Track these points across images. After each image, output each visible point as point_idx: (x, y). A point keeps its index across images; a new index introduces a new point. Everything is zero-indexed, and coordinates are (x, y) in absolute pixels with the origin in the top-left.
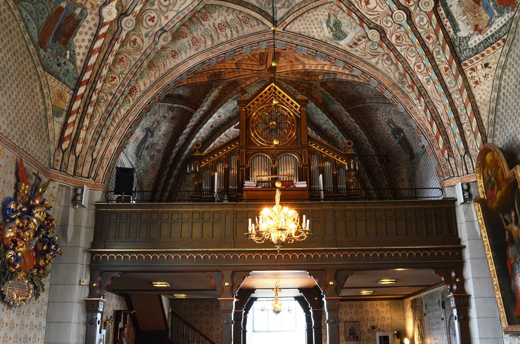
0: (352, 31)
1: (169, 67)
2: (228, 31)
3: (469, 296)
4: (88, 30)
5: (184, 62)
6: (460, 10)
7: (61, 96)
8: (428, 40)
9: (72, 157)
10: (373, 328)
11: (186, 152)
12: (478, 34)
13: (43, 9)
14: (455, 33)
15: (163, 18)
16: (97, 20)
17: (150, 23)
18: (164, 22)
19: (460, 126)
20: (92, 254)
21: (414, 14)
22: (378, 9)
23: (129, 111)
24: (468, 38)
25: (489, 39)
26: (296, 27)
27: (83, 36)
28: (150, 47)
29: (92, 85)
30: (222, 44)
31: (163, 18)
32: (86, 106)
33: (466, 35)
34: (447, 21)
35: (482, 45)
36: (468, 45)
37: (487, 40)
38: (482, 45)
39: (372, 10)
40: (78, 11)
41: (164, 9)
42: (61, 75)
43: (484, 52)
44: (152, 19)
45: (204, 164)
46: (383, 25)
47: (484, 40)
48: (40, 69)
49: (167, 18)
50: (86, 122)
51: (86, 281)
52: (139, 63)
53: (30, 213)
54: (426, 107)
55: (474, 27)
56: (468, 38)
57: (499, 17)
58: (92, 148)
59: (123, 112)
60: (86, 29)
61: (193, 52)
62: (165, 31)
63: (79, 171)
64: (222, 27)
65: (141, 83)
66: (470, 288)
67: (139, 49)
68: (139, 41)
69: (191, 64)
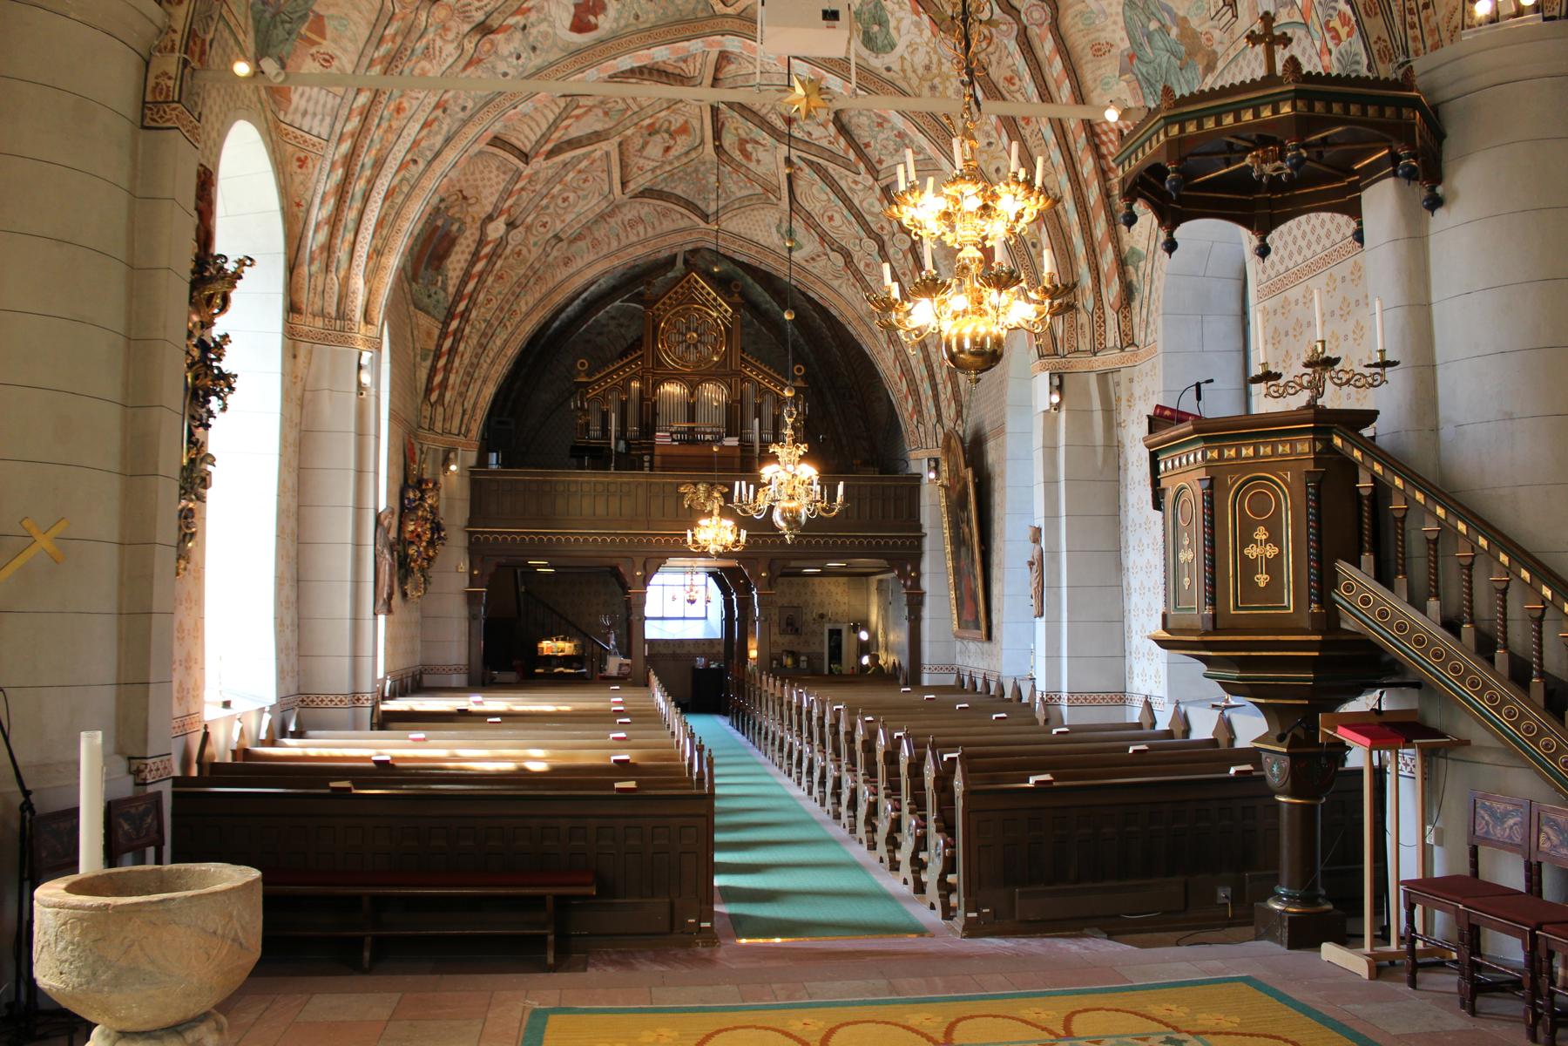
0: (809, 245)
1: (559, 278)
2: (641, 228)
3: (922, 594)
5: (579, 272)
7: (429, 334)
10: (822, 616)
16: (477, 237)
17: (542, 230)
18: (559, 226)
19: (934, 387)
20: (471, 534)
21: (888, 244)
23: (506, 342)
26: (733, 224)
28: (538, 259)
29: (465, 316)
30: (631, 245)
32: (456, 342)
40: (455, 227)
42: (431, 309)
45: (591, 394)
46: (850, 247)
48: (412, 308)
50: (456, 363)
51: (464, 566)
52: (524, 281)
53: (422, 499)
54: (896, 357)
58: (463, 395)
59: (499, 342)
61: (592, 257)
63: (448, 426)
64: (632, 224)
65: (522, 303)
66: (926, 584)
67: (524, 261)
68: (525, 251)
69: (589, 274)
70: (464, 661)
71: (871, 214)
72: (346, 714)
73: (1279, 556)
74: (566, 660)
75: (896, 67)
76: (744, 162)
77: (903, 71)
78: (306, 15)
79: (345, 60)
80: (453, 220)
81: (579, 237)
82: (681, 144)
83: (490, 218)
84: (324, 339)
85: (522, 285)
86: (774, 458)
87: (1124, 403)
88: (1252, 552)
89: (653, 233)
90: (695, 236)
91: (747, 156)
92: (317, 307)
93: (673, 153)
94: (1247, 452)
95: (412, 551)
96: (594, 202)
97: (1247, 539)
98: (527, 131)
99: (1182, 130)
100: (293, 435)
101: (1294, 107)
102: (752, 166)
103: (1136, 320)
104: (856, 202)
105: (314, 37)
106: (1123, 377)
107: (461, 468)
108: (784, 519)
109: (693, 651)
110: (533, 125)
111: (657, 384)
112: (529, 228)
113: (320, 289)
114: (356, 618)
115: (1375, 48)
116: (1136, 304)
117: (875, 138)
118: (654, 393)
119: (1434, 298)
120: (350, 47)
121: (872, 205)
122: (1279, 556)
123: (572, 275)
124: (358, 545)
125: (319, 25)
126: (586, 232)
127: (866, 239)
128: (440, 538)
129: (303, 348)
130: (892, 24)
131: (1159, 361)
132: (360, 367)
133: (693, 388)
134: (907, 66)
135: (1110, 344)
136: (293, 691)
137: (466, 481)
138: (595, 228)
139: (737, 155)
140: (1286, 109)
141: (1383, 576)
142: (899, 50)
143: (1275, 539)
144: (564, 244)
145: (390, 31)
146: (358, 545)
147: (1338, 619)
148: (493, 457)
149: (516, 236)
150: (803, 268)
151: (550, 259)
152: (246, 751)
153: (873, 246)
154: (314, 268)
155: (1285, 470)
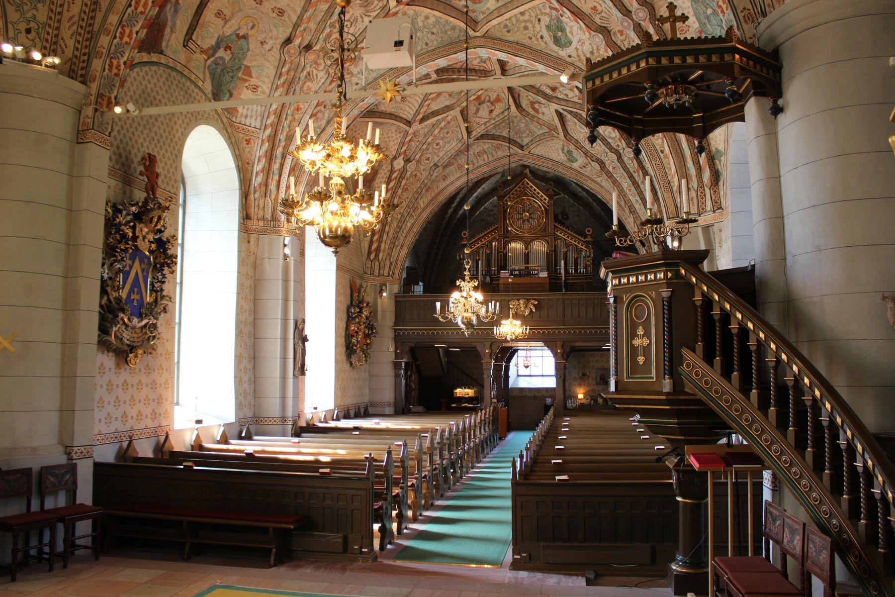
1: (441, 187)
2: (485, 156)
5: (452, 183)
9: (377, 263)
11: (455, 221)
16: (390, 168)
18: (436, 159)
20: (396, 330)
23: (413, 224)
26: (539, 150)
28: (427, 178)
30: (481, 166)
44: (428, 159)
46: (602, 158)
50: (385, 237)
51: (392, 349)
53: (361, 312)
54: (635, 221)
58: (389, 255)
59: (409, 225)
61: (458, 175)
62: (438, 166)
63: (382, 272)
64: (480, 154)
65: (421, 202)
67: (419, 180)
68: (419, 174)
69: (458, 184)
70: (392, 400)
71: (611, 138)
72: (278, 428)
73: (650, 344)
74: (470, 400)
75: (574, 54)
76: (536, 114)
77: (578, 56)
78: (240, 67)
79: (264, 87)
81: (449, 164)
82: (499, 108)
83: (395, 158)
84: (265, 232)
85: (419, 193)
86: (459, 289)
87: (717, 245)
88: (637, 342)
89: (489, 160)
90: (517, 158)
91: (537, 111)
92: (260, 216)
93: (495, 113)
94: (633, 279)
95: (354, 340)
96: (454, 144)
97: (633, 335)
98: (408, 109)
99: (594, 84)
100: (248, 283)
101: (647, 63)
102: (540, 116)
103: (722, 193)
105: (246, 77)
106: (716, 228)
107: (390, 294)
108: (463, 323)
109: (546, 395)
110: (411, 105)
111: (506, 244)
112: (418, 162)
113: (262, 206)
114: (284, 378)
115: (741, 15)
116: (721, 183)
118: (505, 248)
119: (782, 173)
120: (267, 80)
122: (650, 344)
123: (448, 186)
124: (285, 339)
125: (248, 72)
126: (452, 161)
127: (609, 153)
128: (372, 333)
129: (253, 238)
130: (568, 30)
131: (730, 217)
132: (285, 245)
133: (527, 244)
134: (580, 53)
135: (708, 209)
136: (249, 414)
137: (393, 301)
138: (458, 158)
139: (531, 111)
140: (643, 64)
141: (709, 358)
142: (574, 44)
143: (647, 334)
144: (440, 169)
145: (285, 69)
146: (285, 339)
147: (683, 386)
148: (419, 289)
149: (411, 167)
150: (579, 172)
151: (433, 177)
152: (201, 447)
153: (614, 157)
154: (256, 196)
155: (652, 290)
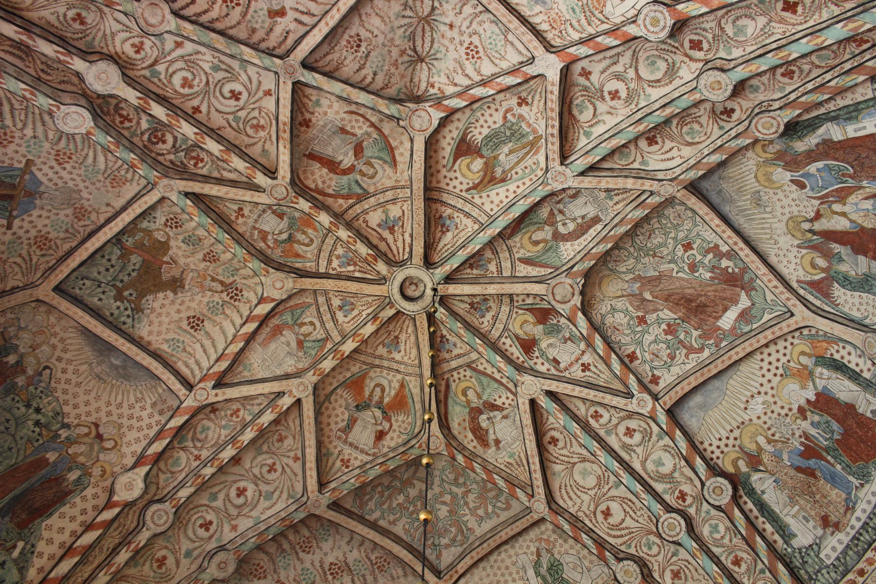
4: (77, 514)
6: (783, 497)
8: (736, 569)
12: (833, 533)
13: (10, 449)
14: (786, 542)
15: (227, 528)
17: (202, 532)
18: (228, 535)
21: (697, 521)
22: (629, 522)
24: (816, 546)
25: (861, 534)
27: (65, 523)
31: (227, 528)
33: (811, 542)
34: (764, 523)
35: (850, 553)
36: (821, 560)
37: (858, 539)
38: (850, 553)
39: (616, 527)
40: (73, 476)
41: (233, 512)
43: (861, 565)
44: (206, 525)
47: (851, 540)
49: (234, 528)
55: (821, 522)
56: (816, 546)
57: (862, 485)
60: (75, 512)
68: (170, 561)
76: (480, 450)
80: (72, 463)
82: (401, 426)
91: (480, 435)
93: (389, 442)
96: (281, 505)
98: (200, 354)
102: (490, 454)
104: (637, 466)
110: (207, 343)
112: (181, 514)
117: (640, 343)
121: (659, 463)
139: (469, 440)
